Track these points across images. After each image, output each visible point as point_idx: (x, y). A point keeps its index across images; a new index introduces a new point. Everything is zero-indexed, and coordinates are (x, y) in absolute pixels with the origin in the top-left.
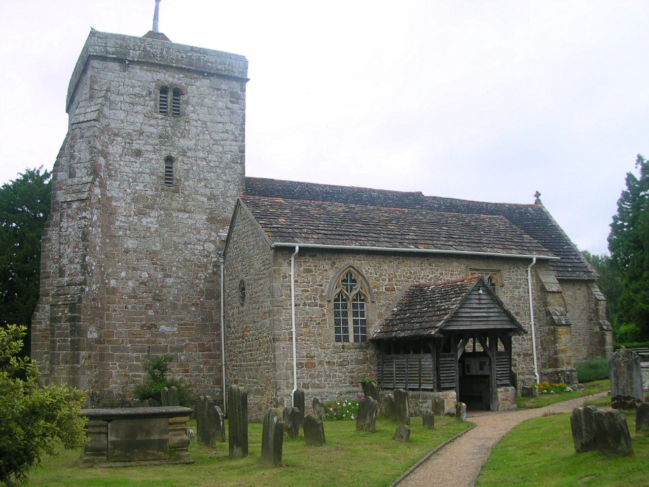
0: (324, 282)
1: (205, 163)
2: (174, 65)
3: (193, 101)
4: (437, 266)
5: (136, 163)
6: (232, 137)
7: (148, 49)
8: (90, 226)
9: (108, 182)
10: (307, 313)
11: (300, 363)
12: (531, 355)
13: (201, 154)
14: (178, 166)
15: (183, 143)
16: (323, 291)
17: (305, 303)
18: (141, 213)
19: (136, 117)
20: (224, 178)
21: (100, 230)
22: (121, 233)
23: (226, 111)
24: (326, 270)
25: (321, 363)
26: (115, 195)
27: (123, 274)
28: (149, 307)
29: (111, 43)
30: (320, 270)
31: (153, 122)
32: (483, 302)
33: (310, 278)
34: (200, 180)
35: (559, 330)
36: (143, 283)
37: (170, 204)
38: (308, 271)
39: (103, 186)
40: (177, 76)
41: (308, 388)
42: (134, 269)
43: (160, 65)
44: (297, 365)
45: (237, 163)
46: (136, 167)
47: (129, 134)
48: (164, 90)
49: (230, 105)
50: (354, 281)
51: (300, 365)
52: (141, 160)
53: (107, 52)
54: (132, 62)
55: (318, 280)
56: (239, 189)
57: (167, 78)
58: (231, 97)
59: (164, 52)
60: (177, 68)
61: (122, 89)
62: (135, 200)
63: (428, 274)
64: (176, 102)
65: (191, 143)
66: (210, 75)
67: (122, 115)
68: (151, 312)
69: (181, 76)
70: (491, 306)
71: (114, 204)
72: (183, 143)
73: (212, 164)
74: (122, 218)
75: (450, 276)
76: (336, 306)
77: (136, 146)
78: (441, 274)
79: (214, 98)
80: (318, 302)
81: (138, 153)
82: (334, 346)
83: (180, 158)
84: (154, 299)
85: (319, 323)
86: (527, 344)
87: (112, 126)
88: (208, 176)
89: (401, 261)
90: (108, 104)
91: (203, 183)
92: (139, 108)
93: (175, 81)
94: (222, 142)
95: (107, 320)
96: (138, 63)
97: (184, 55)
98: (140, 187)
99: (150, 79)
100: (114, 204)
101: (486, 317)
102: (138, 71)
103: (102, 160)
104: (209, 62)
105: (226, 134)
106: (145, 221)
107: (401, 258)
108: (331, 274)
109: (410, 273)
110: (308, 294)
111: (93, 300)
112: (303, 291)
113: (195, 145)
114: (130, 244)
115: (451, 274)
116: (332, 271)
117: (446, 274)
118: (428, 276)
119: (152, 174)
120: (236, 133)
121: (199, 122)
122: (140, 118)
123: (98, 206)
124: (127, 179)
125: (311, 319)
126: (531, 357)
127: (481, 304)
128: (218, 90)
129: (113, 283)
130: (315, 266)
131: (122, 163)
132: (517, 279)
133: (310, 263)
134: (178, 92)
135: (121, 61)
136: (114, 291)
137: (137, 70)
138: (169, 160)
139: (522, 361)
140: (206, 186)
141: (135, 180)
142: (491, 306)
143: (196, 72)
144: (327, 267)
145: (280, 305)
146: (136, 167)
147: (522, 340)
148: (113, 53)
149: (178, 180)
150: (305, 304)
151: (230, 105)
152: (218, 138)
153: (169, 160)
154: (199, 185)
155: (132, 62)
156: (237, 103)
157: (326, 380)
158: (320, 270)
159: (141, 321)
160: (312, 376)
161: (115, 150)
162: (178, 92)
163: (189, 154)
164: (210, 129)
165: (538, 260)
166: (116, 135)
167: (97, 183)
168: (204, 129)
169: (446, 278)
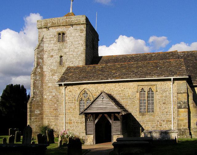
3: (68, 36)
6: (81, 45)
7: (53, 22)
8: (35, 81)
12: (171, 121)
13: (71, 53)
15: (65, 50)
18: (53, 75)
22: (47, 82)
25: (74, 122)
26: (46, 70)
27: (48, 94)
28: (55, 103)
31: (56, 45)
32: (104, 101)
33: (71, 94)
34: (70, 62)
36: (54, 96)
37: (61, 71)
39: (42, 68)
42: (51, 92)
43: (57, 26)
47: (49, 51)
48: (59, 34)
49: (80, 34)
50: (87, 94)
53: (42, 26)
57: (60, 30)
58: (81, 31)
62: (51, 71)
67: (47, 45)
68: (56, 105)
69: (64, 28)
71: (45, 73)
72: (65, 50)
73: (74, 56)
76: (80, 103)
77: (51, 54)
80: (74, 102)
81: (52, 56)
82: (79, 117)
84: (57, 101)
85: (74, 109)
86: (169, 116)
88: (73, 60)
90: (43, 42)
92: (52, 42)
97: (64, 21)
101: (106, 107)
103: (41, 61)
106: (54, 77)
108: (79, 92)
114: (50, 85)
117: (126, 89)
122: (52, 44)
125: (71, 108)
128: (76, 30)
132: (165, 88)
134: (63, 34)
135: (46, 28)
137: (51, 29)
138: (61, 57)
142: (109, 103)
149: (64, 63)
151: (80, 34)
153: (61, 57)
157: (76, 128)
159: (53, 107)
162: (63, 34)
163: (67, 54)
165: (173, 79)
166: (46, 52)
167: (39, 68)
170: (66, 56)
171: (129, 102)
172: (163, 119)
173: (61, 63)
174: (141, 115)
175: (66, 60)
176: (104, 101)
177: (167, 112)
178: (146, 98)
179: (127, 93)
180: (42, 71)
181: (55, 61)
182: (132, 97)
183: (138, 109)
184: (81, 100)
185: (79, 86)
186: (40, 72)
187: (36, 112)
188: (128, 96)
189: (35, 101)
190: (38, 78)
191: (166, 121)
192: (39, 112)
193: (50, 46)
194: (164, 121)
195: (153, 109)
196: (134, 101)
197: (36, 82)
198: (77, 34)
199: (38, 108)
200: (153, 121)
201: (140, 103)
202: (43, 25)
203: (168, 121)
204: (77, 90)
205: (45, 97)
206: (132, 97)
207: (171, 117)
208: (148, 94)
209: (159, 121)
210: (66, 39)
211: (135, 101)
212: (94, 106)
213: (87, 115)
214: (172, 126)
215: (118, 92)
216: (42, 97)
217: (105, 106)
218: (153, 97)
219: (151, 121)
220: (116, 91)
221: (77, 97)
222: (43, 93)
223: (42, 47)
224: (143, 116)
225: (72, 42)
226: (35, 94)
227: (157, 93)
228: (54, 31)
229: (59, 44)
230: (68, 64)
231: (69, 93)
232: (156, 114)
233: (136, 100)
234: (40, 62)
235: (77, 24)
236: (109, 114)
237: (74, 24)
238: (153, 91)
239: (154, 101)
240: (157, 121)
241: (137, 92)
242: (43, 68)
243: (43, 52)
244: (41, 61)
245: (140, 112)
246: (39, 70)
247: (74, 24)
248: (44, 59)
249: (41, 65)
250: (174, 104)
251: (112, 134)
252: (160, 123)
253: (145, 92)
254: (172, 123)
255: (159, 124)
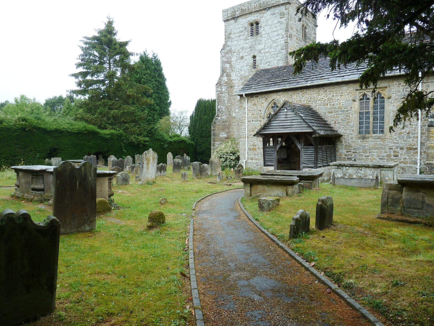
0: (262, 109)
1: (269, 54)
2: (253, 11)
4: (330, 92)
5: (241, 62)
6: (281, 37)
7: (243, 8)
8: (220, 93)
9: (231, 74)
10: (254, 125)
11: (250, 148)
12: (417, 149)
13: (267, 50)
14: (257, 58)
15: (259, 47)
16: (261, 114)
17: (252, 120)
19: (241, 42)
20: (277, 59)
21: (227, 94)
23: (278, 24)
24: (263, 103)
29: (229, 12)
30: (260, 103)
31: (247, 41)
32: (288, 116)
33: (255, 108)
34: (267, 63)
35: (431, 130)
38: (254, 104)
39: (228, 75)
40: (256, 16)
41: (253, 160)
43: (248, 13)
44: (248, 149)
45: (283, 49)
46: (241, 64)
47: (239, 50)
48: (252, 25)
49: (280, 20)
51: (250, 149)
52: (243, 60)
53: (228, 17)
54: (238, 17)
55: (259, 108)
56: (284, 62)
57: (252, 18)
59: (249, 6)
60: (255, 12)
61: (235, 31)
63: (323, 97)
64: (257, 28)
65: (262, 46)
66: (269, 8)
69: (258, 14)
70: (295, 118)
71: (234, 82)
72: (259, 47)
73: (272, 54)
74: (236, 88)
75: (340, 96)
77: (241, 55)
78: (333, 96)
79: (272, 20)
81: (242, 58)
83: (258, 55)
86: (413, 141)
87: (233, 49)
88: (270, 60)
89: (305, 92)
90: (230, 40)
91: (268, 64)
92: (242, 37)
93: (256, 18)
94: (276, 41)
95: (232, 129)
96: (240, 16)
97: (257, 4)
98: (243, 73)
99: (245, 22)
100: (234, 82)
102: (241, 20)
104: (268, 2)
105: (278, 36)
107: (305, 90)
108: (266, 104)
109: (311, 98)
110: (254, 115)
111: (223, 122)
112: (252, 114)
113: (265, 46)
115: (341, 95)
116: (266, 103)
117: (336, 96)
118: (323, 98)
119: (247, 65)
120: (283, 34)
121: (266, 34)
122: (242, 41)
123: (225, 85)
124: (238, 70)
126: (416, 151)
127: (287, 117)
128: (274, 14)
129: (234, 115)
130: (258, 102)
131: (236, 64)
133: (255, 100)
134: (257, 23)
135: (233, 18)
136: (234, 118)
137: (240, 20)
138: (254, 57)
139: (405, 153)
140: (269, 65)
141: (241, 70)
142: (295, 118)
143: (265, 9)
144: (263, 101)
145: (242, 122)
146: (241, 64)
147: (407, 138)
148: (230, 16)
149: (257, 65)
150: (253, 121)
151: (280, 20)
152: (275, 39)
153: (254, 57)
154: (266, 65)
155: (238, 17)
156: (284, 17)
158: (260, 103)
160: (255, 155)
161: (234, 59)
163: (262, 51)
164: (271, 36)
166: (234, 52)
168: (268, 37)
169: (336, 99)
170: (261, 55)
171: (341, 117)
172: (401, 145)
173: (254, 65)
174: (360, 138)
175: (261, 60)
176: (288, 116)
177: (409, 133)
178: (371, 110)
179: (337, 102)
180: (230, 80)
181: (246, 65)
182: (346, 110)
183: (356, 127)
184: (269, 116)
185: (266, 96)
186: (226, 81)
187: (222, 135)
188: (339, 108)
189: (220, 120)
190: (223, 90)
191: (407, 148)
192: (225, 136)
193: (239, 43)
194: (402, 149)
195: (383, 128)
196: (349, 116)
197: (221, 94)
198: (276, 21)
199: (223, 130)
200: (382, 148)
201: (360, 118)
202: (229, 15)
203: (411, 149)
204: (263, 101)
205: (234, 115)
206: (346, 110)
207: (417, 142)
208: (375, 102)
209: (392, 149)
210: (261, 30)
211: (351, 115)
212: (274, 123)
213: (266, 138)
214: (419, 158)
215: (322, 102)
216: (230, 114)
217: (289, 124)
218: (383, 108)
219: (378, 148)
220: (319, 101)
221: (263, 112)
222: (231, 109)
223: (228, 46)
224: (363, 139)
225: (268, 34)
226: (220, 112)
227: (390, 100)
228: (244, 22)
229: (251, 40)
230: (262, 66)
231: (252, 107)
232: (387, 137)
233: (352, 114)
234: (226, 68)
235: (275, 5)
236: (298, 136)
237: (271, 7)
238: (383, 98)
239: (385, 115)
240: (390, 149)
241: (354, 101)
242: (230, 76)
243: (231, 53)
244: (227, 65)
245: (360, 133)
246: (225, 79)
247: (271, 7)
248: (232, 63)
249: (228, 71)
250: (423, 119)
251: (301, 167)
252: (394, 152)
253: (368, 99)
254: (417, 152)
255: (392, 154)
